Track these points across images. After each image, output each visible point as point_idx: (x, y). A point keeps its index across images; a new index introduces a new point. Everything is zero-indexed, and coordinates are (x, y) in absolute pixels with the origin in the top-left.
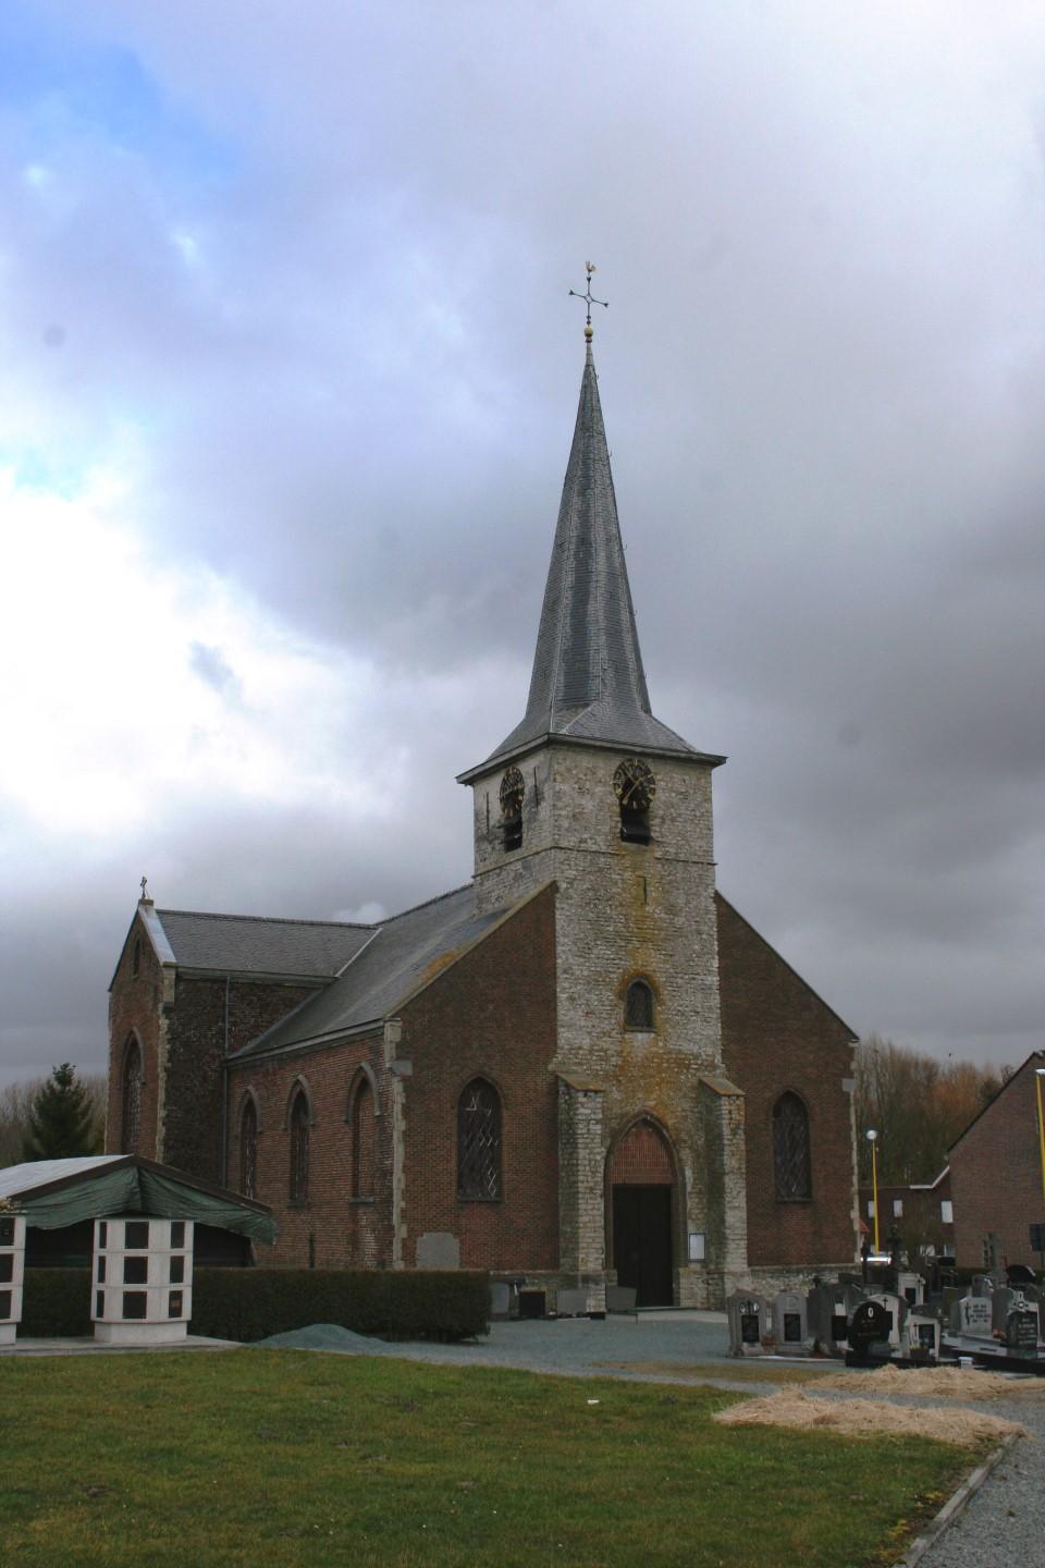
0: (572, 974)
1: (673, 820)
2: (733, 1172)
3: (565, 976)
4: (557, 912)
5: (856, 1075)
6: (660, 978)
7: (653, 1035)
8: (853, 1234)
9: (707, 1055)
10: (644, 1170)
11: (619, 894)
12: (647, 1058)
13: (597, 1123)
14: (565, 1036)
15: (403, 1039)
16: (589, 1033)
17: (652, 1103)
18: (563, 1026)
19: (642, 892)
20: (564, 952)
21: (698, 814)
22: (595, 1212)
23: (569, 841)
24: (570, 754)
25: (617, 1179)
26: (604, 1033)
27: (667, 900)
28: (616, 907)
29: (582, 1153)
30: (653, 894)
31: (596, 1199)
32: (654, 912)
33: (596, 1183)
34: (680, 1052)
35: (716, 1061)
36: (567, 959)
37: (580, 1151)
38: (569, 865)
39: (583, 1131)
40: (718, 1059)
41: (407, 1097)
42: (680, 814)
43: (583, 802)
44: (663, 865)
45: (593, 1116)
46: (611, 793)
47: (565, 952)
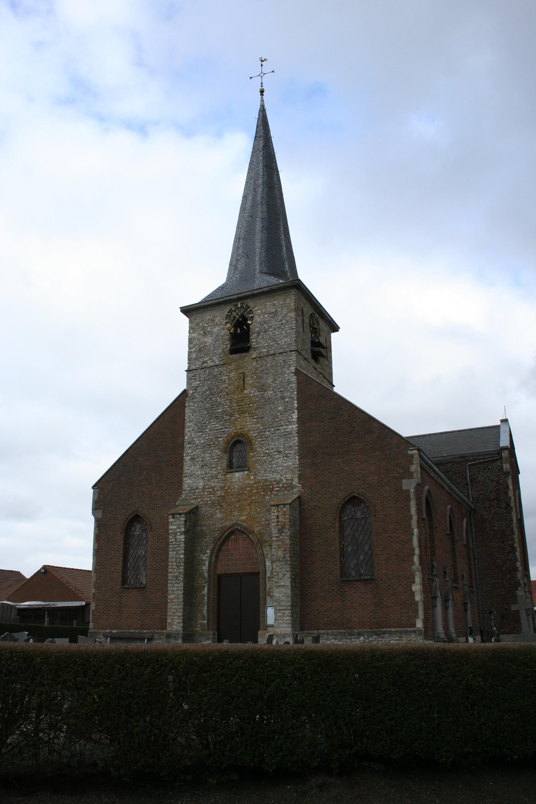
0: (194, 444)
1: (266, 331)
2: (279, 560)
3: (190, 446)
4: (187, 409)
5: (415, 475)
6: (253, 434)
7: (246, 472)
8: (416, 603)
9: (287, 480)
10: (234, 562)
11: (226, 388)
12: (242, 489)
13: (181, 534)
14: (187, 482)
15: (99, 498)
16: (203, 478)
17: (243, 518)
18: (186, 477)
19: (242, 382)
20: (189, 431)
21: (284, 322)
22: (179, 592)
23: (196, 365)
24: (198, 315)
25: (221, 570)
26: (213, 477)
27: (259, 383)
28: (224, 396)
29: (171, 554)
30: (249, 381)
31: (179, 583)
32: (250, 393)
33: (180, 572)
34: (266, 480)
35: (294, 483)
36: (191, 435)
37: (170, 553)
38: (195, 379)
39: (173, 540)
40: (296, 481)
41: (98, 530)
42: (271, 326)
43: (206, 340)
44: (257, 361)
45: (178, 530)
46: (224, 329)
47: (190, 431)
